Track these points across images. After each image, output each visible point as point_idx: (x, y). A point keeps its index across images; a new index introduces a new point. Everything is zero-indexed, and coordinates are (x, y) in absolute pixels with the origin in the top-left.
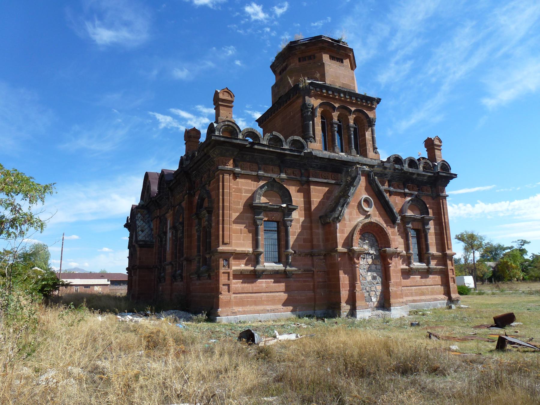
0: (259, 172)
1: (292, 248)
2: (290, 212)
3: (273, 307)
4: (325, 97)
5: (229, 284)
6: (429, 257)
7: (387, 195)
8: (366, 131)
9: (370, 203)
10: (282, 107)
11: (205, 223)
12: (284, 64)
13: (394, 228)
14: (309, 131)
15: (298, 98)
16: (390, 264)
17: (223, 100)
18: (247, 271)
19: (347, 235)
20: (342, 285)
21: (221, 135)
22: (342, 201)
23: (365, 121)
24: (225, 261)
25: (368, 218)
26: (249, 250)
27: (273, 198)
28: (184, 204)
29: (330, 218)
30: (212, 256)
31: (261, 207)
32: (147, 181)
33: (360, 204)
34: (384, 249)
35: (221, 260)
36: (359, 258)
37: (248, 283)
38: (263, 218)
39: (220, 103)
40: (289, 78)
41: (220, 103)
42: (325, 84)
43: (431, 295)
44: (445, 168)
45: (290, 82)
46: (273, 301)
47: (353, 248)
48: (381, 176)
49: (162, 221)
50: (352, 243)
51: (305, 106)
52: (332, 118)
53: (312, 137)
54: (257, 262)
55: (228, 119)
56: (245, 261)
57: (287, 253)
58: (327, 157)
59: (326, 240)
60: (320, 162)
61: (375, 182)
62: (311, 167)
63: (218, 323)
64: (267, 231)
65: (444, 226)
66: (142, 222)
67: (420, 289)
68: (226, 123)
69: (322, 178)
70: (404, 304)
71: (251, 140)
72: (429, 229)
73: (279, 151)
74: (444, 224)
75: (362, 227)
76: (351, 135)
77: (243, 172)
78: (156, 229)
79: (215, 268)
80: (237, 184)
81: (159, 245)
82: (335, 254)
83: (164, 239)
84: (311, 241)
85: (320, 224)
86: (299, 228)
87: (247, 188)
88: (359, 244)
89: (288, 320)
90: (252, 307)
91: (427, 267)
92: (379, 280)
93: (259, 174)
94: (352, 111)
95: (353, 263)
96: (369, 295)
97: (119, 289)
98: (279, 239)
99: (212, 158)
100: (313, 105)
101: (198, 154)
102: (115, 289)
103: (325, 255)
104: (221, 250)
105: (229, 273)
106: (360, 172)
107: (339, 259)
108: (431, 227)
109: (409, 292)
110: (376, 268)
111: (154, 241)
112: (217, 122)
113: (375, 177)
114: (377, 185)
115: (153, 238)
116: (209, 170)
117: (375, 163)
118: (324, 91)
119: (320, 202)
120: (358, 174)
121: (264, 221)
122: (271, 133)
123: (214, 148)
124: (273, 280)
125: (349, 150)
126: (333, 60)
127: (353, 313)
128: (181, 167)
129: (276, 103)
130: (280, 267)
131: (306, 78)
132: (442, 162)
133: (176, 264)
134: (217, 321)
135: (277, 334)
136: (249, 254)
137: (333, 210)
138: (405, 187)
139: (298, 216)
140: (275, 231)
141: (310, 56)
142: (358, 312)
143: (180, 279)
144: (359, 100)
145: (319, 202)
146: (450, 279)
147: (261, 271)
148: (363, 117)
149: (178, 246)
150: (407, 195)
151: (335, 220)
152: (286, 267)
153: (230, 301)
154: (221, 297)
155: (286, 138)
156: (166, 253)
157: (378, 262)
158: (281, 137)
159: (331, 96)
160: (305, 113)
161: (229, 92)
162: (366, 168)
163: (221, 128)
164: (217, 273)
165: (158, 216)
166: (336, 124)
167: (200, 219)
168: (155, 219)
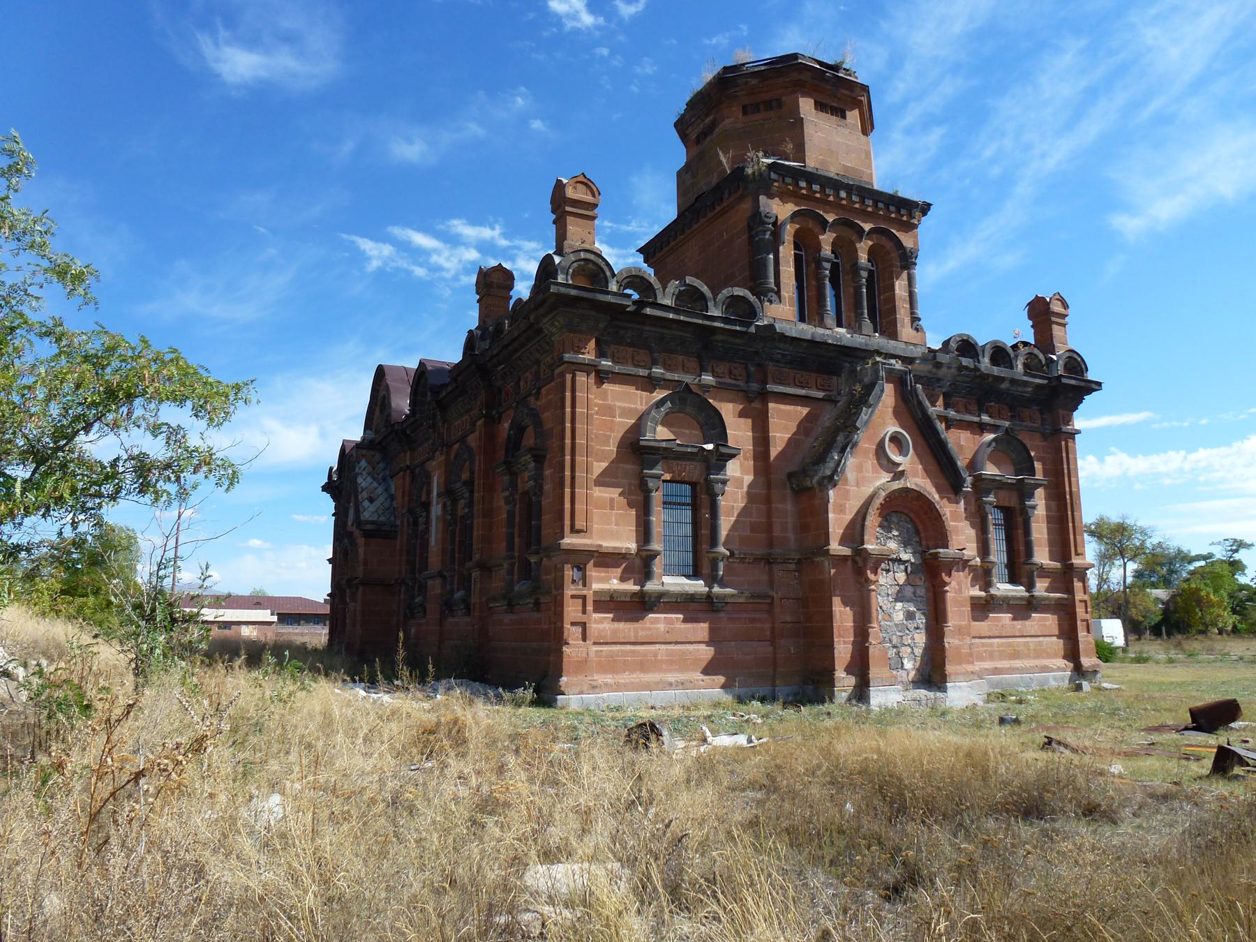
0: (654, 370)
1: (724, 545)
2: (723, 463)
3: (681, 677)
4: (804, 197)
5: (585, 623)
6: (1032, 573)
7: (941, 426)
8: (897, 279)
9: (904, 445)
10: (702, 220)
11: (525, 482)
12: (707, 121)
13: (957, 502)
14: (766, 277)
15: (742, 198)
16: (946, 584)
17: (576, 203)
18: (625, 593)
19: (851, 517)
20: (839, 630)
21: (570, 282)
22: (840, 438)
23: (895, 255)
24: (575, 570)
25: (899, 479)
26: (629, 546)
27: (683, 430)
28: (473, 440)
29: (812, 477)
30: (545, 559)
31: (658, 449)
32: (380, 386)
33: (881, 446)
34: (934, 551)
35: (567, 567)
36: (877, 569)
37: (626, 620)
38: (662, 475)
39: (568, 209)
40: (721, 153)
41: (568, 209)
42: (805, 166)
44: (1074, 367)
45: (724, 160)
46: (681, 663)
47: (865, 546)
48: (930, 383)
49: (419, 478)
50: (863, 536)
51: (757, 218)
52: (818, 247)
53: (772, 290)
54: (647, 575)
55: (587, 246)
56: (619, 570)
57: (713, 555)
58: (809, 337)
59: (803, 528)
60: (791, 348)
61: (917, 396)
62: (772, 360)
63: (561, 708)
64: (670, 503)
65: (1069, 501)
66: (369, 480)
67: (1010, 645)
68: (582, 255)
69: (795, 385)
70: (976, 677)
71: (636, 296)
72: (1034, 507)
73: (700, 322)
74: (1068, 497)
75: (885, 500)
76: (860, 287)
77: (617, 369)
78: (403, 496)
79: (553, 585)
80: (604, 396)
81: (411, 532)
82: (822, 559)
83: (421, 520)
84: (769, 528)
85: (789, 491)
86: (742, 498)
87: (627, 405)
88: (878, 538)
89: (716, 705)
90: (635, 675)
91: (1027, 594)
92: (921, 620)
93: (653, 375)
94: (864, 231)
95: (863, 580)
96: (898, 654)
98: (696, 524)
99: (547, 335)
100: (777, 217)
101: (510, 325)
102: (289, 633)
103: (799, 562)
104: (569, 544)
105: (584, 598)
106: (882, 373)
107: (833, 571)
108: (1039, 503)
109: (985, 651)
110: (914, 593)
111: (398, 522)
112: (559, 251)
113: (918, 385)
114: (920, 403)
115: (395, 517)
116: (538, 362)
117: (917, 352)
118: (803, 184)
119: (790, 439)
120: (877, 377)
121: (664, 481)
122: (681, 278)
123: (554, 313)
124: (681, 616)
125: (856, 321)
126: (822, 111)
127: (861, 693)
128: (471, 355)
129: (687, 209)
130: (698, 586)
131: (761, 154)
132: (1068, 354)
133: (452, 576)
134: (559, 704)
135: (708, 734)
136: (628, 556)
137: (821, 458)
138: (981, 409)
139: (739, 472)
140: (688, 505)
141: (771, 101)
142: (874, 691)
143: (464, 611)
144: (881, 205)
145: (787, 439)
146: (1079, 623)
147: (656, 595)
148: (888, 245)
149: (457, 535)
150: (986, 429)
151: (826, 481)
152: (711, 588)
153: (586, 661)
154: (567, 650)
155: (715, 293)
156: (427, 552)
157: (920, 581)
158: (705, 289)
159: (818, 195)
160: (757, 235)
161: (587, 184)
162: (898, 365)
163: (569, 268)
164: (559, 597)
165: (408, 467)
166: (828, 260)
167: (514, 475)
168: (402, 473)
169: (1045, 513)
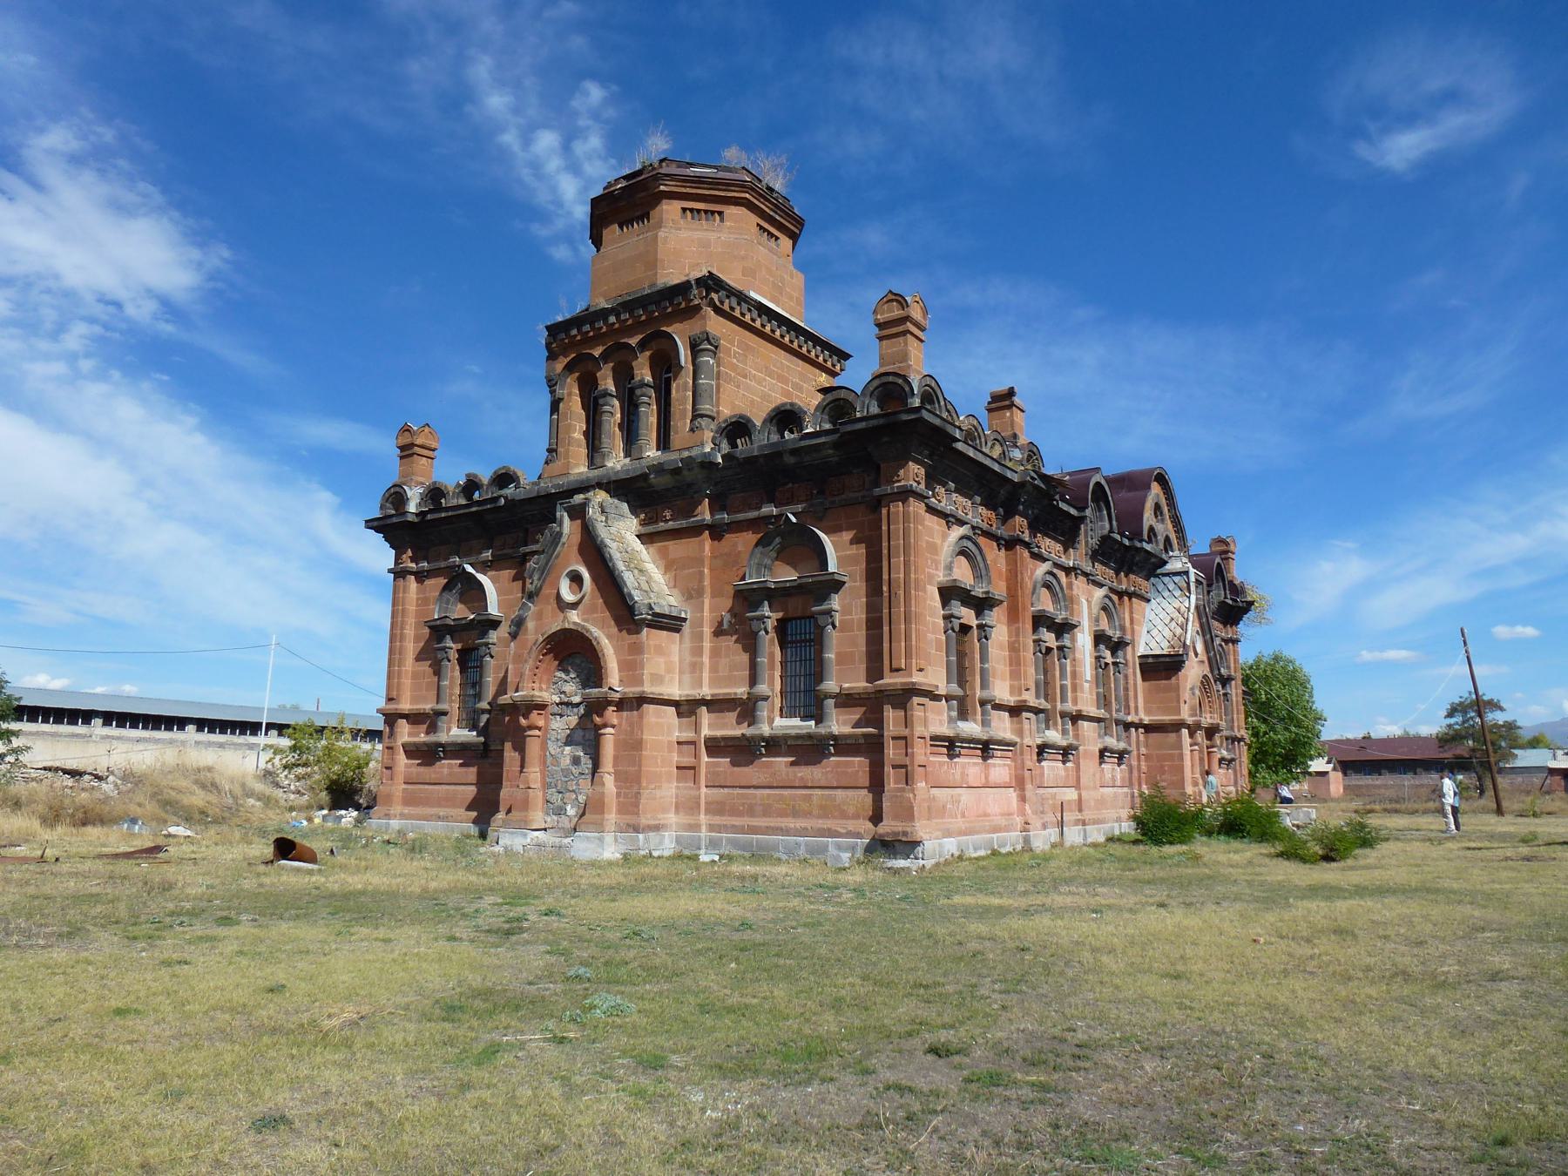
43: (819, 817)
46: (448, 801)
56: (425, 726)
58: (534, 494)
65: (886, 594)
67: (782, 797)
70: (631, 830)
92: (587, 763)
97: (1379, 787)
102: (1367, 786)
110: (584, 736)
146: (888, 770)
159: (591, 334)
169: (864, 616)
